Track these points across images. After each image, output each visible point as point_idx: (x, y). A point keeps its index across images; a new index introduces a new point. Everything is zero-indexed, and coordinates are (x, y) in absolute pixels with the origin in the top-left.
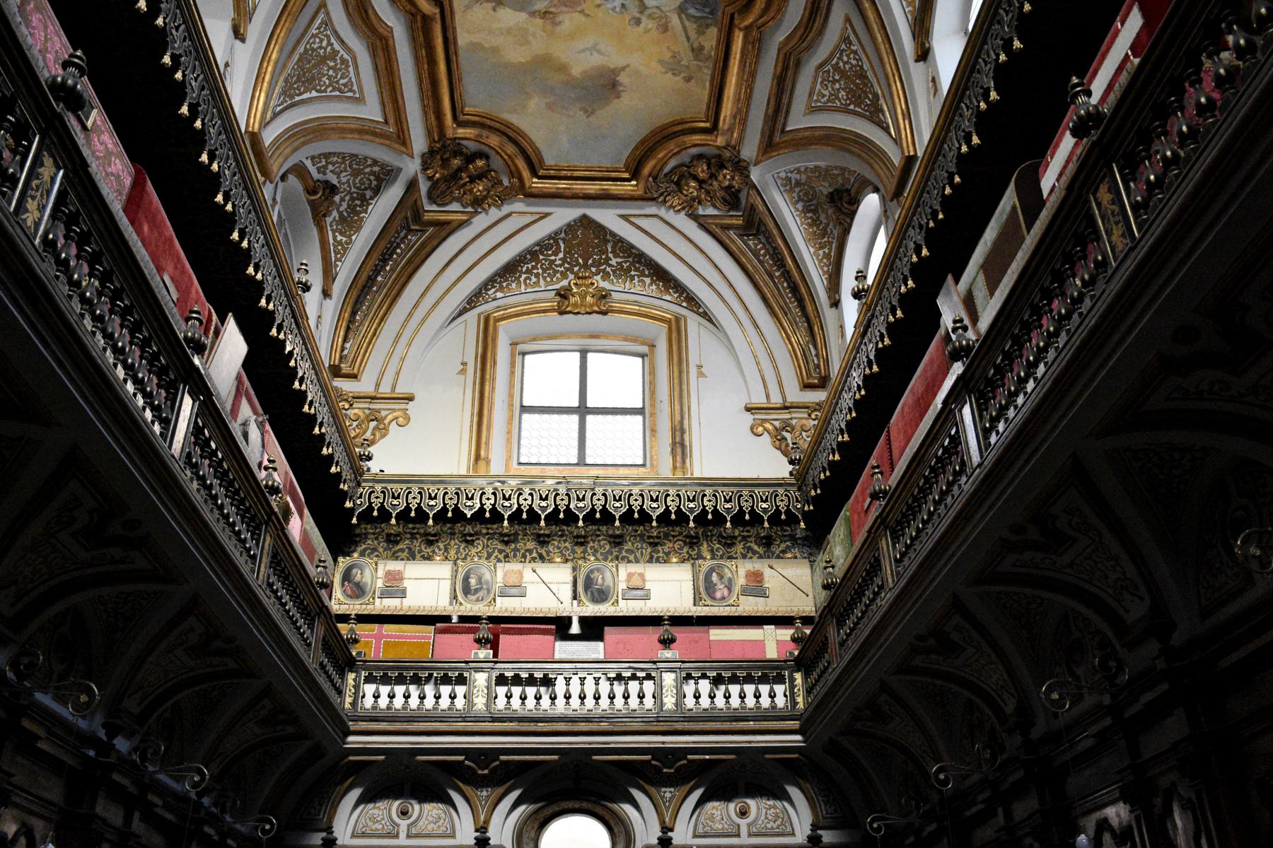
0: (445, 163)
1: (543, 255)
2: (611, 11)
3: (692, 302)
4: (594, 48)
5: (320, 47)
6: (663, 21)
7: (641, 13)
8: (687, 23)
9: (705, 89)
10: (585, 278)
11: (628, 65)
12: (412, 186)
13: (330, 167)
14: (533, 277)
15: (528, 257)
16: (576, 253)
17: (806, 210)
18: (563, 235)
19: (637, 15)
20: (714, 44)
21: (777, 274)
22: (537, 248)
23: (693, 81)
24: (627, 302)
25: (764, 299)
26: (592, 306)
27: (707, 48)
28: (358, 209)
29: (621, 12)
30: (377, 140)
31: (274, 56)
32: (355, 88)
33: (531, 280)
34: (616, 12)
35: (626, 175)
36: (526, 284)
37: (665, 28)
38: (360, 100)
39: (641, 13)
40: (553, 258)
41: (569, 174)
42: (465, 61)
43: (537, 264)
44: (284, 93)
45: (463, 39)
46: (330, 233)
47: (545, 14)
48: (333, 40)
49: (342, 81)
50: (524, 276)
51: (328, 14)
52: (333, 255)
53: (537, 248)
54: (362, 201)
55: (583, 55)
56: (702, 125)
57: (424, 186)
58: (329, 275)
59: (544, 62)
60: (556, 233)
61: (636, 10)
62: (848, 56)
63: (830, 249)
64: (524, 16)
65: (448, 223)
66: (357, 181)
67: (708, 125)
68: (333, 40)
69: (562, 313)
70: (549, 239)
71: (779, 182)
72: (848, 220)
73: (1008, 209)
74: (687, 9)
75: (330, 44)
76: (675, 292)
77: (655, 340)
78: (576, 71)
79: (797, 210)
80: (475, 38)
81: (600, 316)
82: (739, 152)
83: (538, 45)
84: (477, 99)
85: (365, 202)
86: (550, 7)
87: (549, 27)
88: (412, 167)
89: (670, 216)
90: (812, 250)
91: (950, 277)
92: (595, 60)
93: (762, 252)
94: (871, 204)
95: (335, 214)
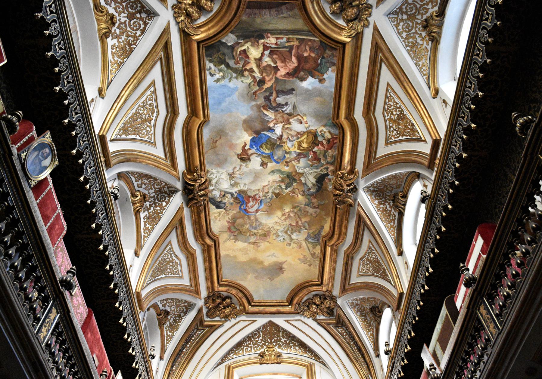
0: (214, 300)
1: (253, 338)
3: (317, 357)
4: (273, 255)
5: (167, 258)
6: (299, 244)
8: (308, 245)
10: (271, 348)
11: (286, 261)
12: (200, 311)
13: (168, 304)
14: (249, 348)
15: (247, 339)
16: (267, 337)
17: (361, 315)
18: (261, 329)
19: (289, 242)
20: (319, 251)
21: (352, 343)
22: (251, 335)
24: (289, 358)
25: (347, 355)
26: (274, 360)
27: (317, 253)
28: (178, 321)
30: (187, 293)
31: (149, 262)
32: (180, 273)
33: (248, 349)
35: (287, 304)
36: (246, 351)
37: (300, 247)
40: (257, 339)
41: (264, 304)
42: (223, 261)
43: (251, 342)
44: (152, 276)
45: (223, 253)
46: (165, 332)
47: (254, 243)
49: (175, 271)
50: (245, 348)
51: (171, 246)
52: (166, 341)
53: (251, 335)
54: (179, 318)
55: (269, 257)
56: (316, 283)
57: (205, 311)
58: (163, 350)
59: (254, 261)
60: (259, 329)
61: (289, 240)
62: (371, 254)
63: (373, 332)
64: (246, 244)
65: (214, 326)
66: (178, 309)
67: (319, 283)
68: (173, 255)
69: (261, 364)
70: (256, 331)
71: (349, 304)
72: (379, 319)
73: (444, 315)
75: (171, 257)
76: (309, 353)
77: (301, 375)
78: (266, 264)
79: (358, 316)
80: (227, 253)
81: (278, 364)
82: (332, 293)
84: (227, 275)
85: (180, 318)
87: (256, 248)
88: (200, 303)
89: (306, 320)
90: (365, 332)
91: (425, 345)
92: (272, 260)
93: (345, 334)
94: (387, 314)
95: (168, 323)
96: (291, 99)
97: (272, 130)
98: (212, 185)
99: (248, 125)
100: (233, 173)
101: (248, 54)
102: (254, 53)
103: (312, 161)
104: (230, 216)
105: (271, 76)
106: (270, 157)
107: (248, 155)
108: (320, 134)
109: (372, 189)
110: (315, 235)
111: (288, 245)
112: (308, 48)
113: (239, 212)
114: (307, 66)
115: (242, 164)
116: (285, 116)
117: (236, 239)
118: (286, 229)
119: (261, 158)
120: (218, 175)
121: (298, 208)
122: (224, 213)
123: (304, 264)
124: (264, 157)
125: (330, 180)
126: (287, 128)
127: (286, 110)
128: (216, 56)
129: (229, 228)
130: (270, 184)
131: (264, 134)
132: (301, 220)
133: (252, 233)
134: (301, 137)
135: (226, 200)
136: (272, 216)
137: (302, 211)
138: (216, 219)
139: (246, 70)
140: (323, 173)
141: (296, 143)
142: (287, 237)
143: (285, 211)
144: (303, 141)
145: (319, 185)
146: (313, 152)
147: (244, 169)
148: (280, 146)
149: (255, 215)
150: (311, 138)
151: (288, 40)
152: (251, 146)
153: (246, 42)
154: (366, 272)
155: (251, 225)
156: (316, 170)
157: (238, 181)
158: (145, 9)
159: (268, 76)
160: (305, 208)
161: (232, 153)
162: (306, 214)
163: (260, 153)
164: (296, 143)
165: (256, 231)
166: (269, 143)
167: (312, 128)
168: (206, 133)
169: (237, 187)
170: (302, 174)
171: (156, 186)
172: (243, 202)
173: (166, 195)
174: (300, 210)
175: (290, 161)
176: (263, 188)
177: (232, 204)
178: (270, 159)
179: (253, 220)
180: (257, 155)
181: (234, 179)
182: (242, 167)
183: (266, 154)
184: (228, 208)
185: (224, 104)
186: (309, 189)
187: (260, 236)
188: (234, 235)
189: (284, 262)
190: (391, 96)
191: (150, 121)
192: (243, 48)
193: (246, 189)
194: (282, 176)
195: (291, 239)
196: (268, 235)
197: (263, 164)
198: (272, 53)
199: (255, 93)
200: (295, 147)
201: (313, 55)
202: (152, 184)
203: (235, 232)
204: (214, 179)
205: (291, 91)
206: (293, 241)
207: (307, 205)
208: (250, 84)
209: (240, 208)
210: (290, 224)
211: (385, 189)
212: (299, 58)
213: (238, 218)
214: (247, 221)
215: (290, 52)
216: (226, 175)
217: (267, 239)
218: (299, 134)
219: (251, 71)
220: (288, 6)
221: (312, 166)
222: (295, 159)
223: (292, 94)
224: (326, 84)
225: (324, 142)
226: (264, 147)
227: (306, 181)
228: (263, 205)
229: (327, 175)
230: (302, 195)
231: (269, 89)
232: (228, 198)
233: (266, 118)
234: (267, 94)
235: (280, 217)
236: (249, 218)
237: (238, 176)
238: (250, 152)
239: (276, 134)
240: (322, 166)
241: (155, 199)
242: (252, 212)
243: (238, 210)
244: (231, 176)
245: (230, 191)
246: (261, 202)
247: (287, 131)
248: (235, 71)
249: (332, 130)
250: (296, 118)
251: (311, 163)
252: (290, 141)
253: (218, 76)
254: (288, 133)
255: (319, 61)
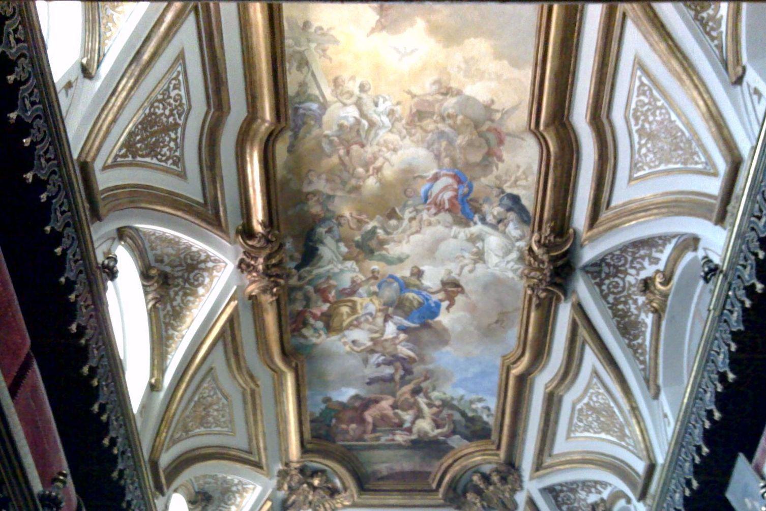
2: (387, 97)
6: (339, 91)
7: (360, 98)
8: (317, 92)
9: (287, 18)
11: (368, 36)
19: (364, 95)
20: (289, 79)
23: (301, 24)
27: (294, 70)
29: (377, 97)
34: (384, 98)
37: (336, 83)
38: (639, 65)
39: (360, 98)
45: (525, 76)
47: (447, 92)
48: (637, 146)
49: (646, 100)
61: (364, 101)
62: (170, 149)
64: (469, 91)
74: (319, 108)
80: (516, 73)
83: (457, 56)
86: (442, 100)
96: (370, 372)
97: (402, 329)
98: (520, 250)
99: (442, 337)
100: (475, 262)
101: (433, 424)
102: (425, 425)
103: (331, 287)
104: (495, 173)
105: (402, 399)
106: (405, 286)
107: (446, 291)
108: (322, 332)
109: (210, 265)
110: (304, 123)
111: (367, 87)
112: (351, 433)
113: (474, 179)
114: (349, 414)
115: (457, 277)
116: (379, 348)
117: (488, 108)
118: (373, 133)
119: (422, 284)
120: (503, 265)
121: (348, 187)
122: (506, 181)
123: (321, 28)
124: (415, 286)
125: (292, 258)
126: (376, 332)
127: (379, 357)
128: (478, 428)
129: (501, 142)
130: (406, 237)
131: (413, 322)
132: (340, 158)
133: (450, 122)
134: (352, 321)
135: (497, 210)
136: (403, 167)
137: (338, 181)
138: (524, 173)
139: (438, 407)
140: (308, 268)
141: (361, 312)
142: (369, 109)
143: (375, 181)
144: (349, 315)
145: (311, 244)
146: (329, 301)
147: (454, 267)
148: (387, 304)
149: (440, 167)
150: (335, 323)
151: (378, 439)
152: (438, 305)
153: (435, 436)
154: (168, 89)
155: (451, 142)
156: (321, 270)
157: (469, 245)
158: (555, 494)
159: (406, 399)
160: (333, 190)
161: (473, 297)
162: (332, 176)
163: (424, 293)
164: (360, 311)
165: (441, 126)
166: (406, 309)
167: (334, 338)
168: (513, 335)
169: (472, 235)
170: (346, 258)
171: (621, 284)
172: (462, 201)
173: (609, 261)
174: (344, 183)
175: (368, 280)
176: (421, 228)
177: (487, 200)
178: (405, 283)
179: (446, 156)
180: (429, 290)
181: (475, 250)
182: (457, 271)
183: (413, 291)
184: (495, 192)
185: (474, 370)
186: (330, 231)
187: (433, 114)
188: (493, 121)
189: (373, 30)
190: (227, 427)
191: (588, 404)
192: (439, 431)
193: (455, 229)
194: (384, 252)
195: (359, 104)
196: (413, 115)
197: (419, 274)
198: (400, 425)
199: (426, 379)
200: (361, 304)
201: (344, 426)
202: (625, 293)
203: (489, 130)
204: (512, 260)
205: (371, 382)
206: (354, 99)
207: (330, 197)
208: (434, 389)
209: (470, 188)
210: (363, 146)
211: (186, 275)
212: (362, 421)
213: (478, 164)
214: (458, 155)
215: (375, 426)
216: (490, 260)
217: (416, 104)
218: (356, 325)
219: (430, 405)
220: (380, 476)
221: (329, 278)
222: (360, 285)
223: (370, 379)
224: (319, 398)
225: (312, 321)
226: (415, 303)
227: (338, 247)
228: (422, 191)
229: (298, 268)
230: (342, 216)
231: (403, 381)
232: (492, 213)
233: (411, 345)
234: (408, 377)
235: (386, 164)
236: (454, 162)
237: (467, 255)
238: (441, 296)
239: (395, 324)
240: (310, 280)
241: (632, 262)
242: (446, 175)
243: (476, 185)
244: (480, 257)
245: (486, 229)
246: (426, 198)
247: (377, 329)
248: (453, 407)
249: (302, 341)
250: (362, 348)
251: (332, 282)
252: (371, 314)
253: (479, 406)
254: (374, 325)
255: (334, 421)
